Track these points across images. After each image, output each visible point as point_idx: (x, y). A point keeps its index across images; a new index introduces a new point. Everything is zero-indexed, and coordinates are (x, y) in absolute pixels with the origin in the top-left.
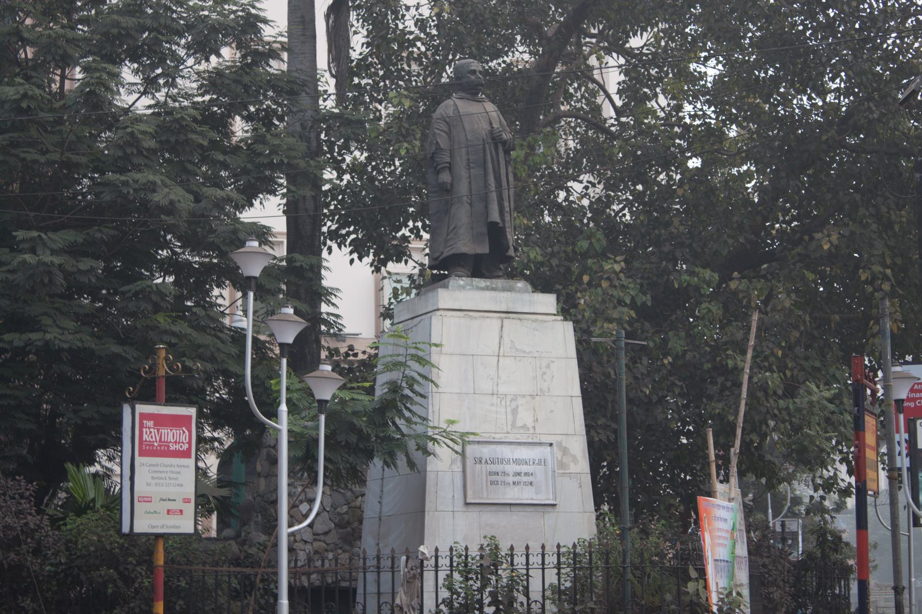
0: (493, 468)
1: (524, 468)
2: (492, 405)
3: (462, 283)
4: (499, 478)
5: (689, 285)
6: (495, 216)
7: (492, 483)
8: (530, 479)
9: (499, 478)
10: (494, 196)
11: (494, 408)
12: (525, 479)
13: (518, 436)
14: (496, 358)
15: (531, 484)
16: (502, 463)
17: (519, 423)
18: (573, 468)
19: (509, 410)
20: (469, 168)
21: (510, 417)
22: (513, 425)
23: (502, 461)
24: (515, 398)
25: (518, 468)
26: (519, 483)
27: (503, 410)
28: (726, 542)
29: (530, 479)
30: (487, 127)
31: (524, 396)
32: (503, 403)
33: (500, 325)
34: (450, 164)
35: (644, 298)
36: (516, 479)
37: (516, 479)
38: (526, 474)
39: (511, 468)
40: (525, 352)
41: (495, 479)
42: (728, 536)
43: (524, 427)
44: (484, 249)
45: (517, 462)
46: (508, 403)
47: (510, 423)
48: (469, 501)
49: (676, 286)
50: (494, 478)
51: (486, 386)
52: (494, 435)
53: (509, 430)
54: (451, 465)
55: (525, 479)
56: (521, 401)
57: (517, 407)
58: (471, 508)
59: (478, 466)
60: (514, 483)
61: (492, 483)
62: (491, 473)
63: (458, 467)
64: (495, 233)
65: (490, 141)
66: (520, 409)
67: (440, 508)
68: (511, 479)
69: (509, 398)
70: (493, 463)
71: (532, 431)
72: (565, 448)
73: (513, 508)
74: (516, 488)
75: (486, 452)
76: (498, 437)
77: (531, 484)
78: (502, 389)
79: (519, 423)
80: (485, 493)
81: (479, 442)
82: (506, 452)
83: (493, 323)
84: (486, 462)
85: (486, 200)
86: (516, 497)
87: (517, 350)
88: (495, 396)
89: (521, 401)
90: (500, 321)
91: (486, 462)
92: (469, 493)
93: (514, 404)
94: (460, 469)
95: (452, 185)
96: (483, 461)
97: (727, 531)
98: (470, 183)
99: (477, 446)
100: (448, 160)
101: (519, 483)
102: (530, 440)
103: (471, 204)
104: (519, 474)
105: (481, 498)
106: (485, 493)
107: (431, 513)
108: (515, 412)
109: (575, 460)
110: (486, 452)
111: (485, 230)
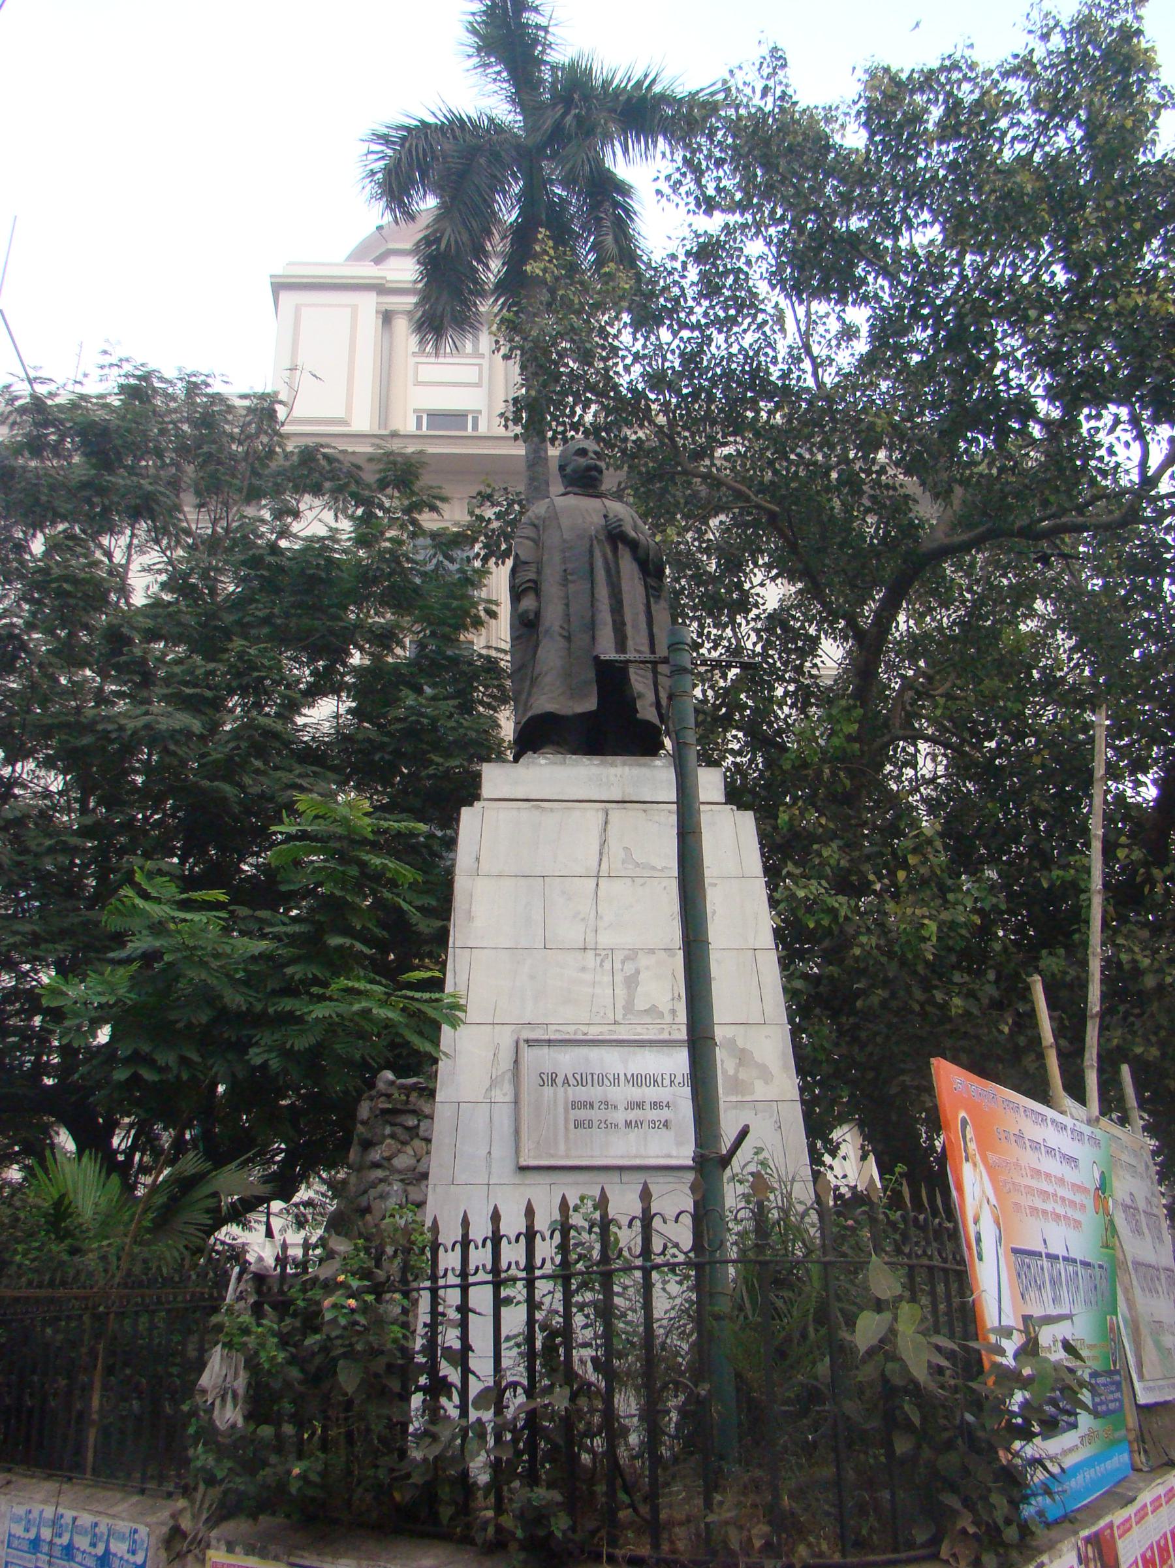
0: (582, 1094)
1: (651, 1093)
2: (583, 969)
3: (543, 761)
4: (595, 1115)
5: (1063, 882)
6: (608, 653)
7: (578, 1124)
8: (665, 1114)
9: (595, 1115)
10: (605, 616)
11: (587, 977)
12: (654, 1115)
13: (639, 1029)
14: (593, 882)
15: (666, 1124)
16: (601, 1083)
17: (641, 1004)
18: (761, 1091)
19: (619, 978)
20: (565, 582)
21: (621, 992)
22: (629, 1007)
23: (601, 1079)
24: (632, 954)
25: (636, 1093)
26: (638, 1124)
27: (607, 979)
28: (1077, 1215)
29: (665, 1114)
30: (603, 522)
31: (652, 951)
32: (607, 965)
33: (601, 821)
34: (535, 582)
35: (994, 900)
36: (633, 1115)
37: (633, 1115)
38: (656, 1105)
39: (621, 1094)
40: (654, 868)
41: (584, 1117)
42: (1089, 1202)
43: (652, 1010)
44: (590, 704)
45: (636, 1080)
46: (617, 966)
47: (620, 1003)
48: (523, 1163)
49: (1045, 885)
50: (582, 1114)
51: (572, 934)
52: (584, 1029)
53: (619, 1018)
54: (490, 1089)
55: (654, 1115)
56: (644, 961)
57: (638, 972)
58: (531, 1177)
59: (548, 1091)
60: (628, 1124)
61: (578, 1124)
62: (575, 1105)
63: (503, 1095)
64: (611, 679)
65: (602, 537)
66: (641, 977)
67: (461, 1178)
68: (620, 1116)
69: (619, 956)
70: (581, 1083)
71: (668, 1018)
72: (743, 1050)
73: (626, 1177)
74: (633, 1135)
75: (566, 1061)
76: (594, 1032)
77: (666, 1124)
78: (606, 939)
79: (641, 1004)
80: (562, 1146)
81: (549, 1042)
82: (611, 1061)
83: (592, 817)
84: (566, 1081)
85: (592, 627)
86: (634, 1151)
87: (637, 865)
88: (590, 954)
89: (644, 961)
90: (601, 815)
91: (566, 1081)
92: (527, 1144)
93: (629, 968)
94: (509, 1098)
95: (538, 614)
96: (560, 1080)
97: (1078, 1188)
98: (567, 605)
99: (545, 1050)
100: (532, 576)
101: (638, 1124)
102: (665, 1036)
103: (568, 639)
104: (639, 1105)
105: (552, 1156)
106: (562, 1146)
107: (439, 1189)
108: (632, 982)
109: (765, 1074)
110: (566, 1061)
111: (591, 674)
